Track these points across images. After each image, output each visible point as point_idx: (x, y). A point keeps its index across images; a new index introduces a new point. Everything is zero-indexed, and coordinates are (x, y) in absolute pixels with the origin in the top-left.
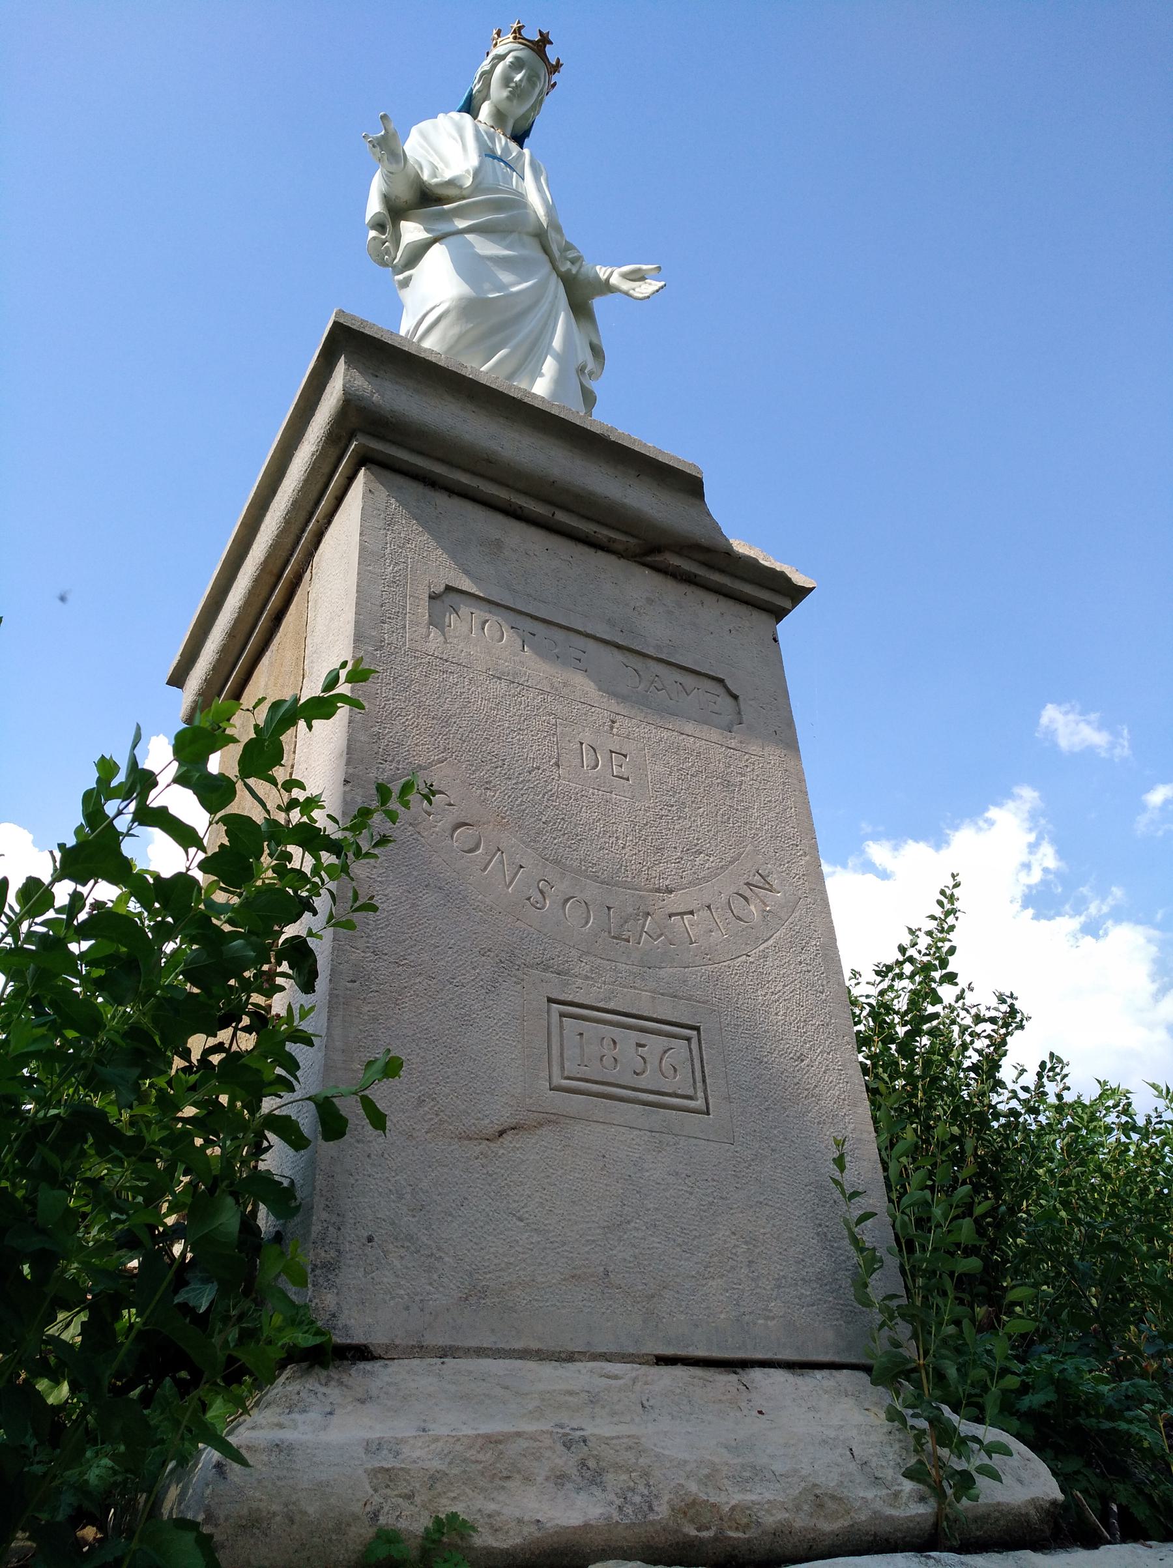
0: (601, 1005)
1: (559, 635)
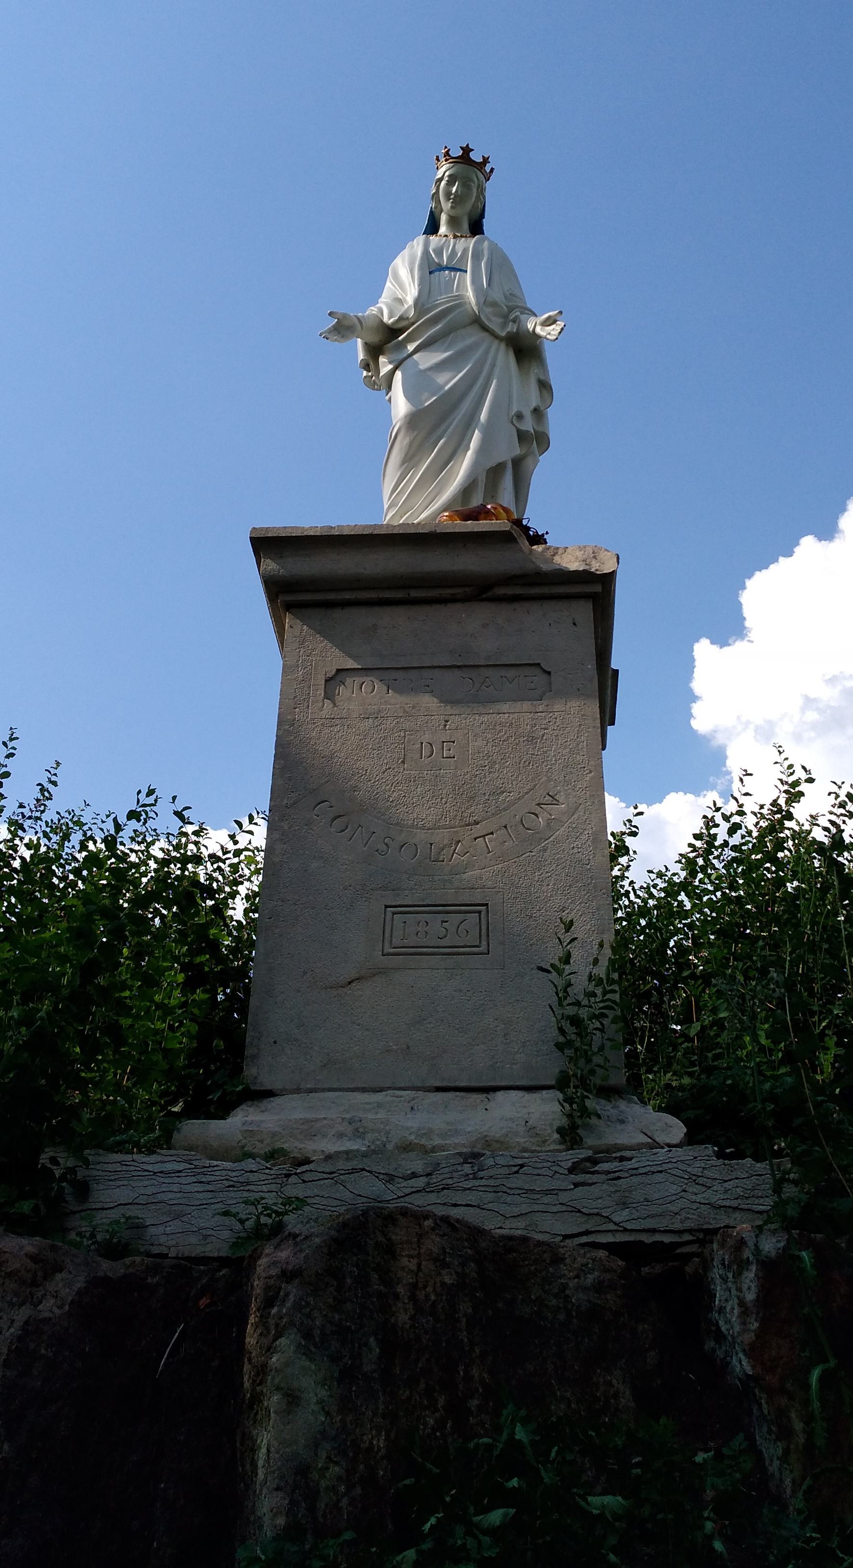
0: (421, 903)
1: (413, 674)
